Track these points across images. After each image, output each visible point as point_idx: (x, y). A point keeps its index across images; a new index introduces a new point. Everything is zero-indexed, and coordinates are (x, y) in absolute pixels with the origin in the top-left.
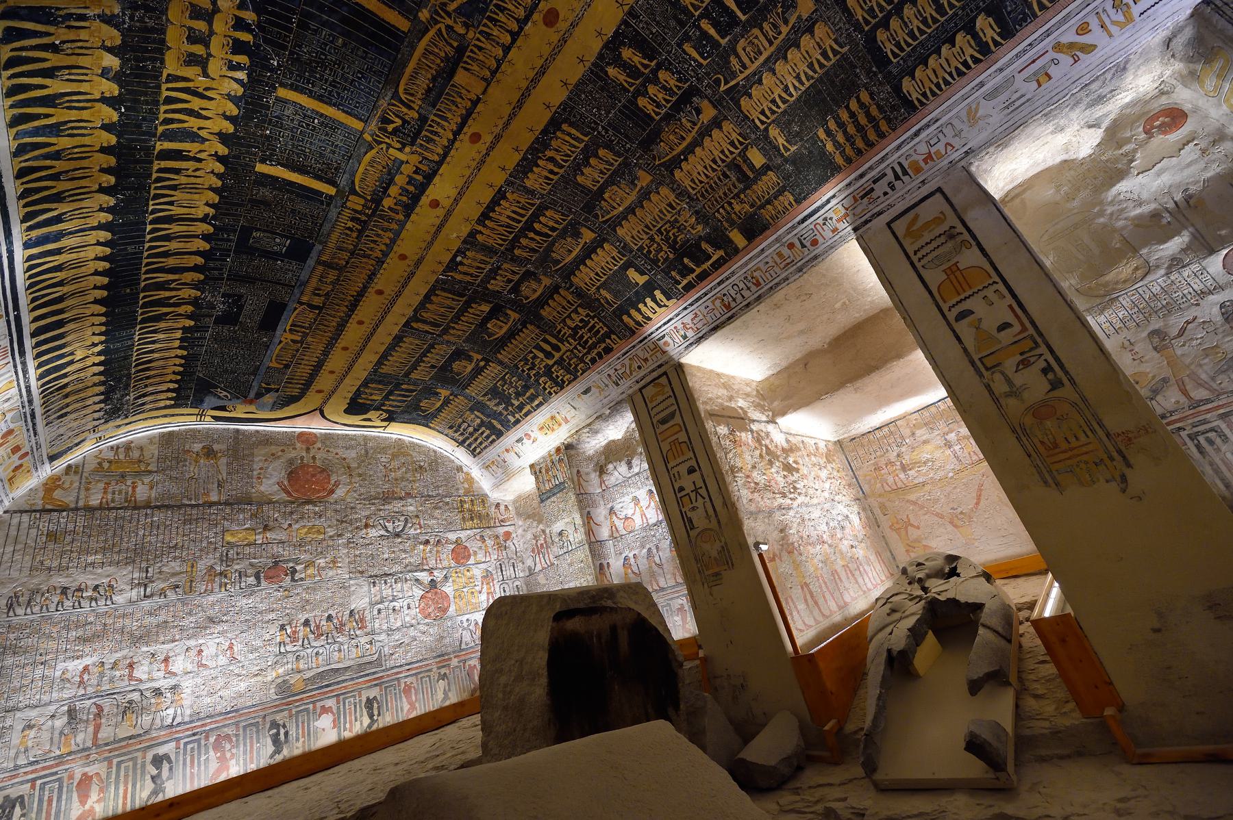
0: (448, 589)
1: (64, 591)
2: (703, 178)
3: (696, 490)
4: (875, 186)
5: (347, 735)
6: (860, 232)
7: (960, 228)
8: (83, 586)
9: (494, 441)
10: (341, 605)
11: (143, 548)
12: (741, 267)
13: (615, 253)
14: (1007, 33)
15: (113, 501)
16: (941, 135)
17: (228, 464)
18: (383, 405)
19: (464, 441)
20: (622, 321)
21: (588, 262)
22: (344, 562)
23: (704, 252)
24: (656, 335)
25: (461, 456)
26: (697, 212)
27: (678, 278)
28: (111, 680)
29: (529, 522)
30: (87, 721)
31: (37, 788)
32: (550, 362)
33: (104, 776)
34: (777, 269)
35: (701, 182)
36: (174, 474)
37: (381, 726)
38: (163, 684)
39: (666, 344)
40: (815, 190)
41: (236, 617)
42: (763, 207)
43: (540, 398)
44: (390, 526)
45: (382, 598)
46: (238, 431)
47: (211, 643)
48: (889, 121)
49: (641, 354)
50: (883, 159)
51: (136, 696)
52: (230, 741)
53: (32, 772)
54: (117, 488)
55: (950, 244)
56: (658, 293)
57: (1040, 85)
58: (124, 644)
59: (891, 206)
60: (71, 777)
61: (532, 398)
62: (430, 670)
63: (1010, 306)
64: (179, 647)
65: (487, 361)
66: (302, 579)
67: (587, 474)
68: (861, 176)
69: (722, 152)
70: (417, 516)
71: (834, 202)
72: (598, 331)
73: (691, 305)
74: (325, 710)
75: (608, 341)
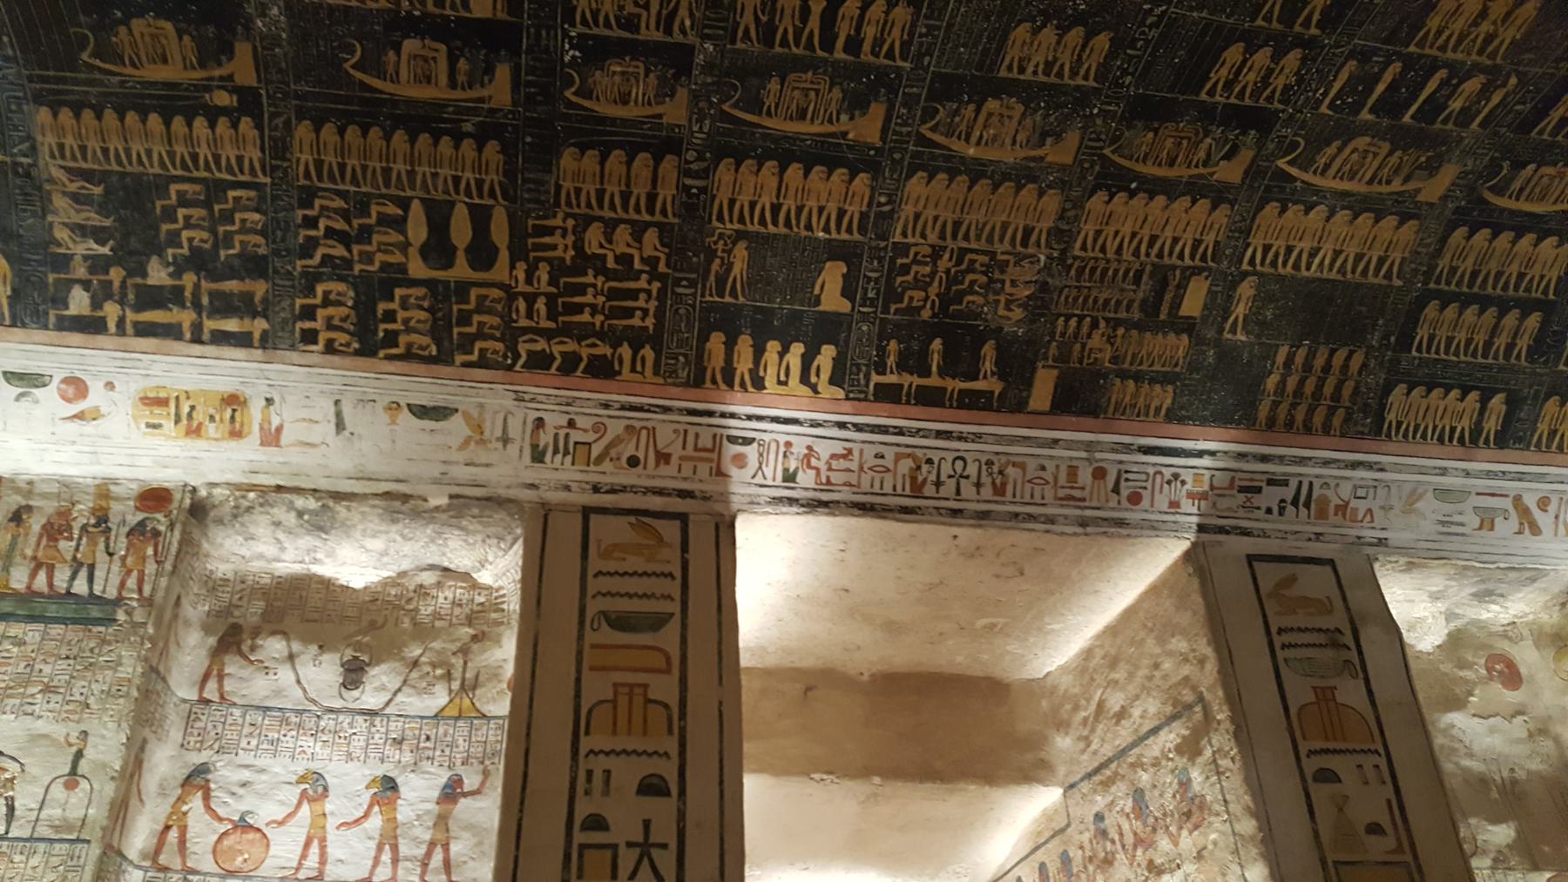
2: (1111, 247)
3: (645, 848)
4: (1266, 489)
6: (1205, 537)
7: (1348, 639)
12: (1000, 439)
13: (854, 210)
14: (1503, 439)
16: (1371, 495)
20: (704, 338)
21: (794, 171)
23: (977, 358)
24: (737, 427)
26: (1044, 287)
27: (891, 361)
32: (417, 268)
34: (1049, 492)
35: (1103, 250)
39: (740, 461)
40: (1204, 422)
42: (1123, 375)
48: (1347, 420)
49: (665, 436)
50: (1302, 461)
55: (1329, 653)
56: (828, 353)
57: (1480, 528)
59: (1264, 534)
61: (225, 306)
63: (1389, 802)
65: (248, 103)
67: (187, 623)
68: (1264, 459)
69: (1176, 240)
71: (1206, 462)
72: (629, 313)
73: (858, 428)
75: (625, 351)
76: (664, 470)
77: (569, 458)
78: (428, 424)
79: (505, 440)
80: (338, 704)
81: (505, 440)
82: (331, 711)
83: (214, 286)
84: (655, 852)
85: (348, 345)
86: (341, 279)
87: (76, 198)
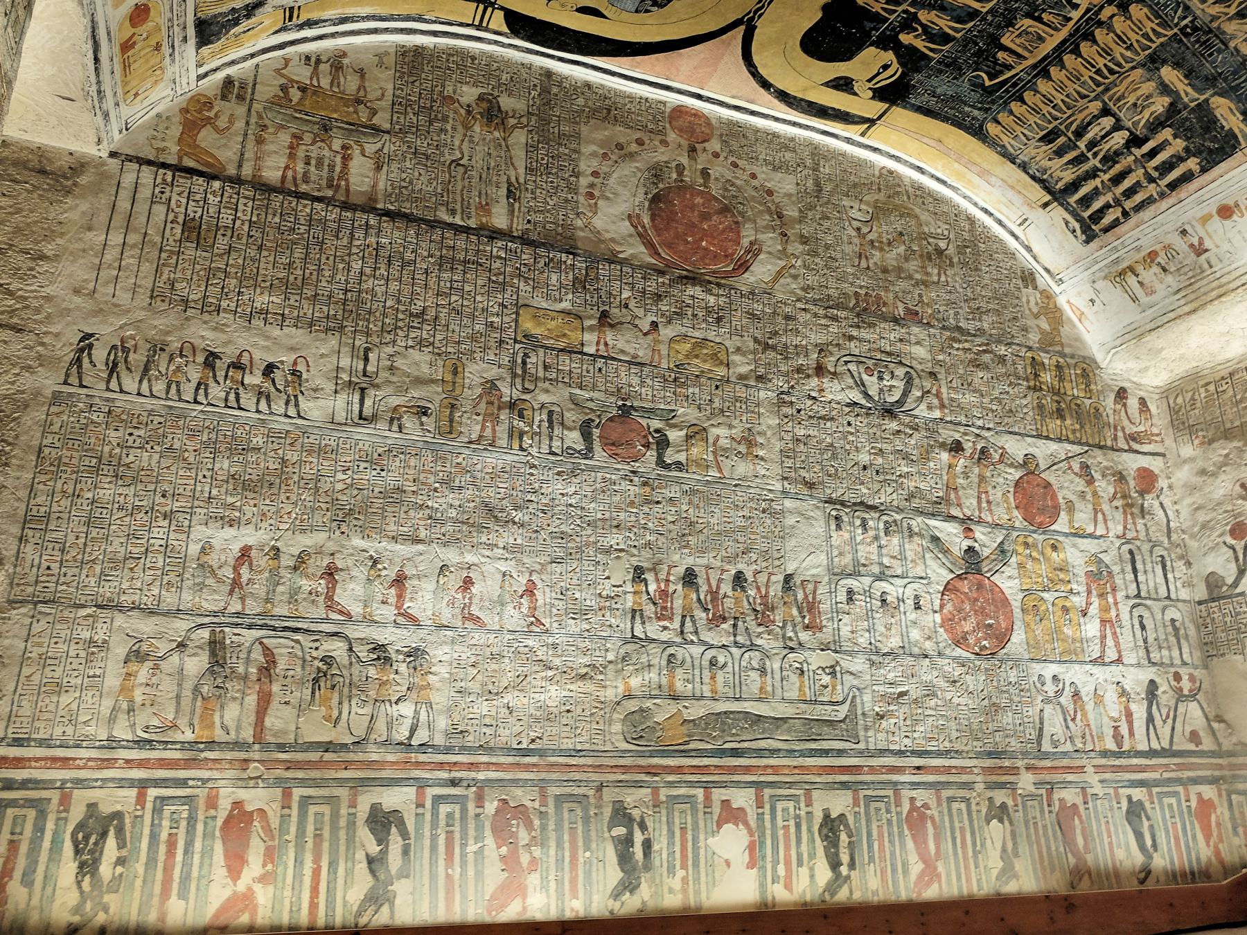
0: (1008, 582)
1: (211, 359)
5: (781, 895)
8: (245, 360)
9: (1187, 177)
10: (765, 555)
11: (359, 301)
15: (306, 179)
17: (530, 148)
18: (909, 23)
19: (1074, 186)
22: (771, 448)
25: (1039, 239)
28: (293, 598)
29: (1222, 449)
30: (245, 678)
31: (149, 806)
33: (275, 823)
36: (422, 144)
37: (857, 896)
38: (396, 638)
41: (542, 520)
44: (872, 382)
45: (856, 563)
46: (549, 74)
47: (489, 568)
51: (337, 649)
52: (529, 826)
53: (142, 764)
54: (314, 152)
58: (318, 518)
60: (212, 803)
62: (968, 786)
64: (429, 557)
66: (679, 466)
70: (933, 375)
74: (731, 814)
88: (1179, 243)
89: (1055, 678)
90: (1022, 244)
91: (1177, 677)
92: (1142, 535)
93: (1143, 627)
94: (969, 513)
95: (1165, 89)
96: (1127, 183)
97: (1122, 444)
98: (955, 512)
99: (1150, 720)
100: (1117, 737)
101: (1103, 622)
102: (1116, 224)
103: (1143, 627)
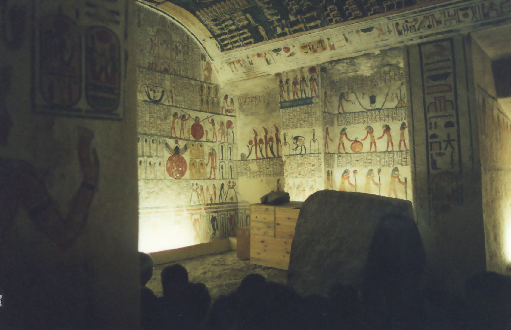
0: (187, 156)
3: (449, 141)
9: (250, 43)
43: (319, 22)
44: (151, 93)
49: (437, 16)
61: (309, 20)
76: (440, 26)
77: (409, 32)
78: (368, 33)
79: (390, 31)
80: (371, 108)
81: (390, 31)
82: (369, 110)
83: (305, 16)
84: (451, 142)
85: (340, 20)
86: (332, 4)
87: (268, 8)
88: (246, 60)
89: (197, 184)
90: (203, 46)
91: (230, 182)
92: (226, 141)
93: (222, 168)
94: (177, 136)
95: (247, 19)
96: (234, 39)
97: (224, 113)
98: (173, 135)
99: (221, 194)
100: (211, 200)
101: (212, 168)
102: (230, 49)
103: (222, 168)
